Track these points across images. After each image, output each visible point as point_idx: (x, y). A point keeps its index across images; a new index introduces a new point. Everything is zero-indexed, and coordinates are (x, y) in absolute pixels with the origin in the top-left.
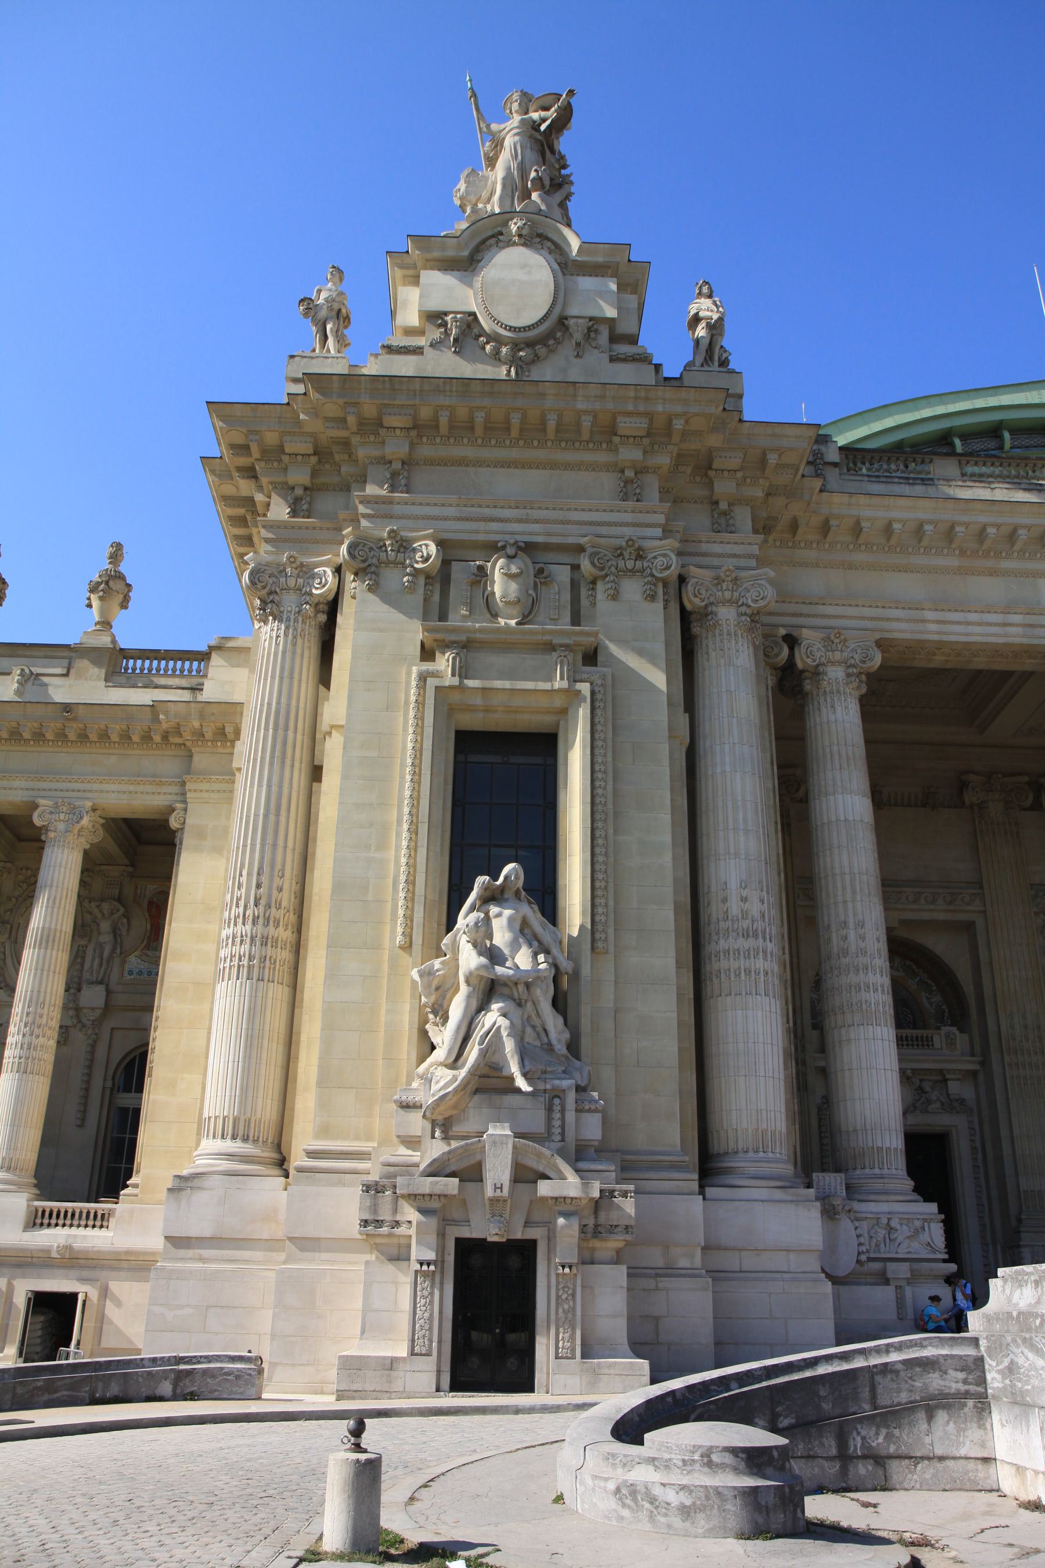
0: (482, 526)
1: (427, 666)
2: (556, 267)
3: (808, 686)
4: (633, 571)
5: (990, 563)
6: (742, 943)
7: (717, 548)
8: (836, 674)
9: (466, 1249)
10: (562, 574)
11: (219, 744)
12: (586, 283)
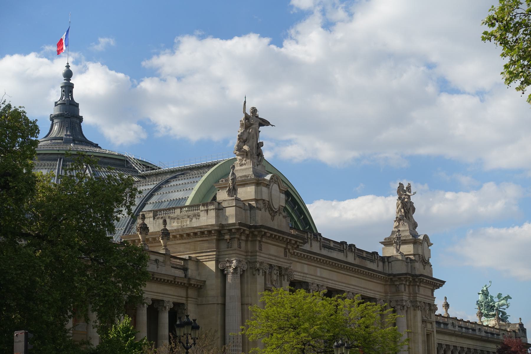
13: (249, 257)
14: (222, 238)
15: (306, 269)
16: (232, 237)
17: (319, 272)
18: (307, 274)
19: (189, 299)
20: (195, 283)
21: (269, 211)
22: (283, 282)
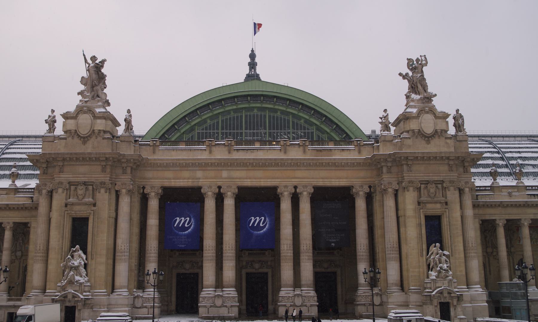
0: (76, 178)
1: (66, 209)
2: (92, 118)
3: (147, 196)
4: (103, 187)
5: (186, 169)
6: (120, 254)
7: (123, 177)
8: (153, 194)
9: (67, 307)
10: (90, 188)
12: (99, 121)
15: (199, 174)
17: (225, 174)
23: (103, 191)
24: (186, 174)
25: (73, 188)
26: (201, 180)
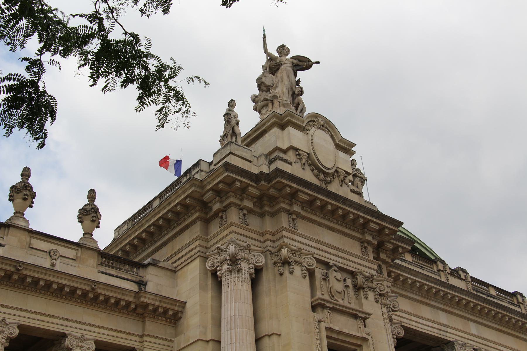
10: (349, 282)
11: (160, 318)
13: (268, 243)
14: (212, 214)
15: (443, 318)
16: (225, 204)
17: (473, 328)
18: (447, 326)
19: (146, 338)
20: (157, 303)
21: (312, 171)
22: (364, 300)
23: (371, 295)
24: (426, 312)
25: (319, 273)
26: (449, 330)
